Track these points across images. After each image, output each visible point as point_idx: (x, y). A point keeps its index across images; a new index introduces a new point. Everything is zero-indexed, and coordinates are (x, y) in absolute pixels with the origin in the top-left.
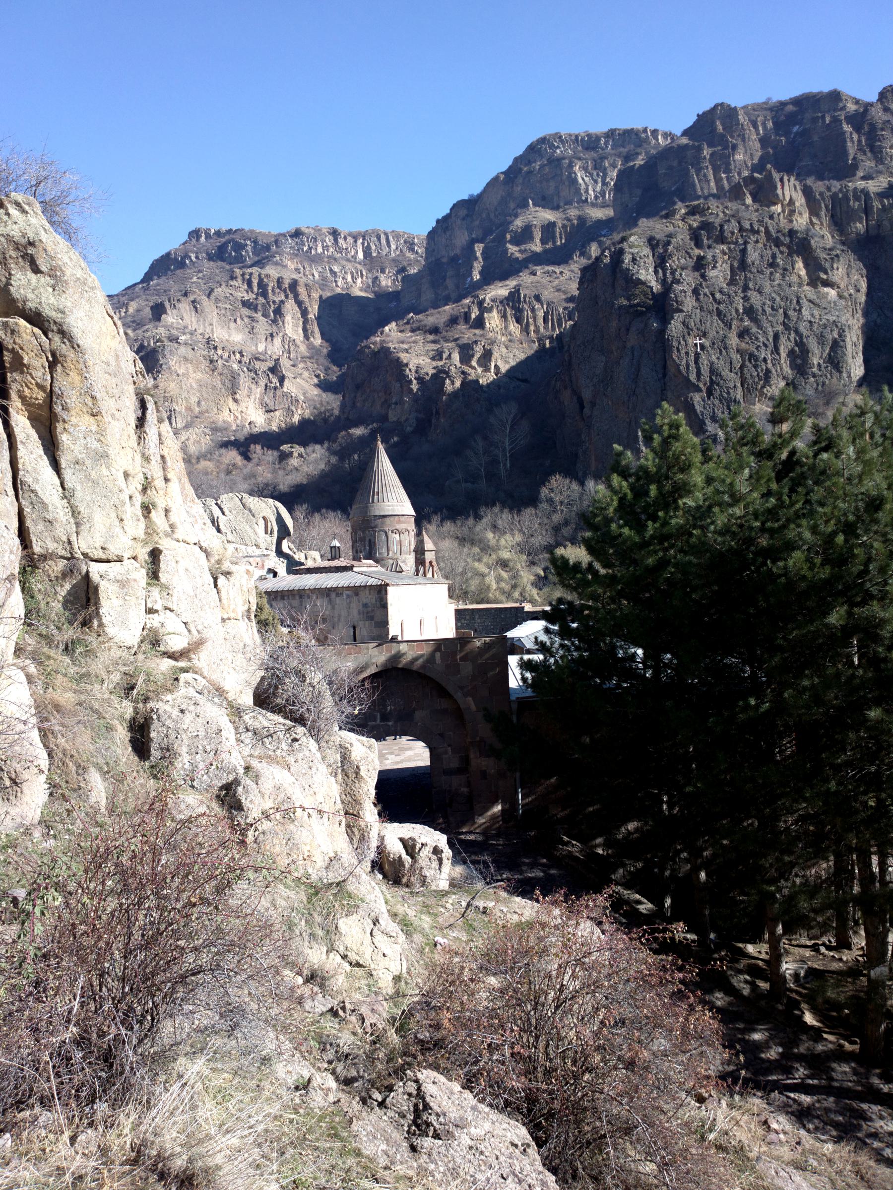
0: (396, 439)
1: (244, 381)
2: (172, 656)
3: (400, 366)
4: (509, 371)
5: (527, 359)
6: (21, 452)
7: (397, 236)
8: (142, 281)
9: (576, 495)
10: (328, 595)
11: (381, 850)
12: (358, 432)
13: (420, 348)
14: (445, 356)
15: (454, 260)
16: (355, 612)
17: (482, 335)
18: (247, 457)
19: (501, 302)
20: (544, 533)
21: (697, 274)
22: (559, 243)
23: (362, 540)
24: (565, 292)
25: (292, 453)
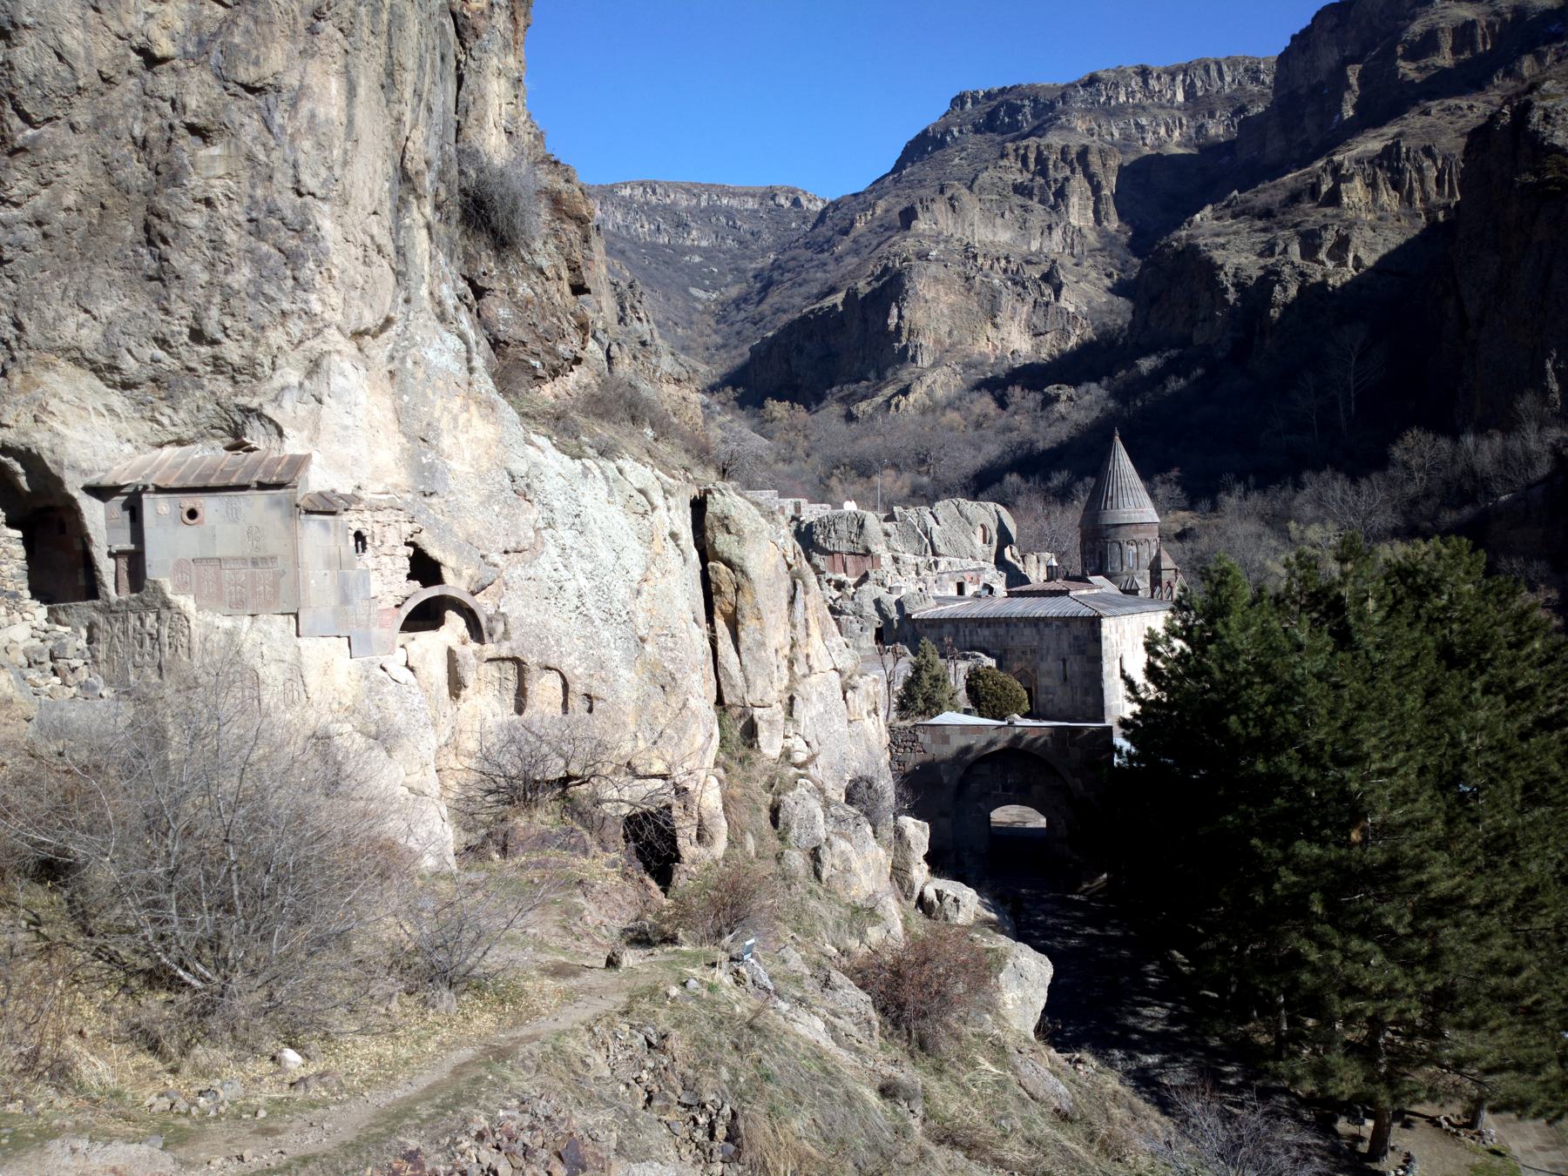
0: (1199, 371)
1: (1007, 300)
2: (798, 766)
3: (1212, 268)
4: (1378, 263)
5: (1408, 242)
6: (721, 646)
7: (1234, 63)
8: (893, 172)
10: (1036, 625)
11: (922, 893)
12: (1146, 364)
13: (1243, 241)
14: (1278, 250)
15: (1315, 90)
16: (1065, 646)
17: (1337, 216)
18: (1002, 404)
19: (1370, 162)
20: (1390, 511)
22: (1481, 49)
23: (1092, 552)
25: (1058, 396)
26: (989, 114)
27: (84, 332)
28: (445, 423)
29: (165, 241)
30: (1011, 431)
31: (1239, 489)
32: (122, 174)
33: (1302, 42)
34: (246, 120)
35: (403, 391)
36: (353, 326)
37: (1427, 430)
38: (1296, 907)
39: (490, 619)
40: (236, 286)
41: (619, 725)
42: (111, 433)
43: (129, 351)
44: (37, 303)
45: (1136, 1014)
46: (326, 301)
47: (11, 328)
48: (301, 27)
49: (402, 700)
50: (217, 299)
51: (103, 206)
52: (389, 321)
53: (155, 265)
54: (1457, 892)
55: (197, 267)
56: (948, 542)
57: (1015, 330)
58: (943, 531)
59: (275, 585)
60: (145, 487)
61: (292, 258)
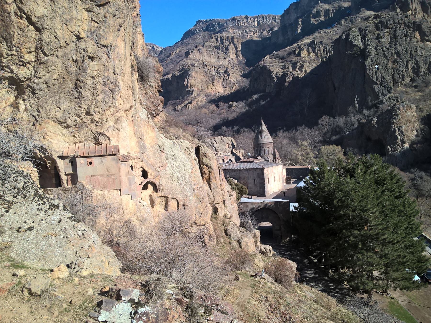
0: (268, 99)
1: (216, 78)
3: (270, 72)
5: (318, 66)
7: (270, 17)
8: (181, 41)
9: (332, 122)
10: (247, 171)
11: (261, 249)
12: (255, 97)
13: (278, 65)
14: (286, 68)
15: (291, 24)
16: (255, 176)
17: (300, 59)
18: (218, 107)
21: (377, 41)
23: (257, 150)
24: (332, 40)
26: (206, 26)
27: (57, 113)
28: (144, 134)
29: (81, 88)
30: (221, 114)
31: (282, 131)
32: (70, 70)
33: (287, 12)
34: (103, 55)
35: (135, 125)
36: (124, 109)
37: (328, 116)
38: (355, 246)
39: (159, 186)
40: (99, 100)
41: (192, 212)
42: (63, 141)
43: (69, 118)
44: (44, 105)
45: (306, 273)
46: (120, 103)
47: (36, 112)
48: (116, 29)
49: (145, 210)
50: (94, 103)
51: (64, 78)
52: (131, 106)
53: (78, 94)
54: (391, 240)
55: (89, 95)
56: (220, 148)
57: (218, 86)
58: (218, 145)
59: (114, 182)
60: (77, 156)
61: (112, 91)
